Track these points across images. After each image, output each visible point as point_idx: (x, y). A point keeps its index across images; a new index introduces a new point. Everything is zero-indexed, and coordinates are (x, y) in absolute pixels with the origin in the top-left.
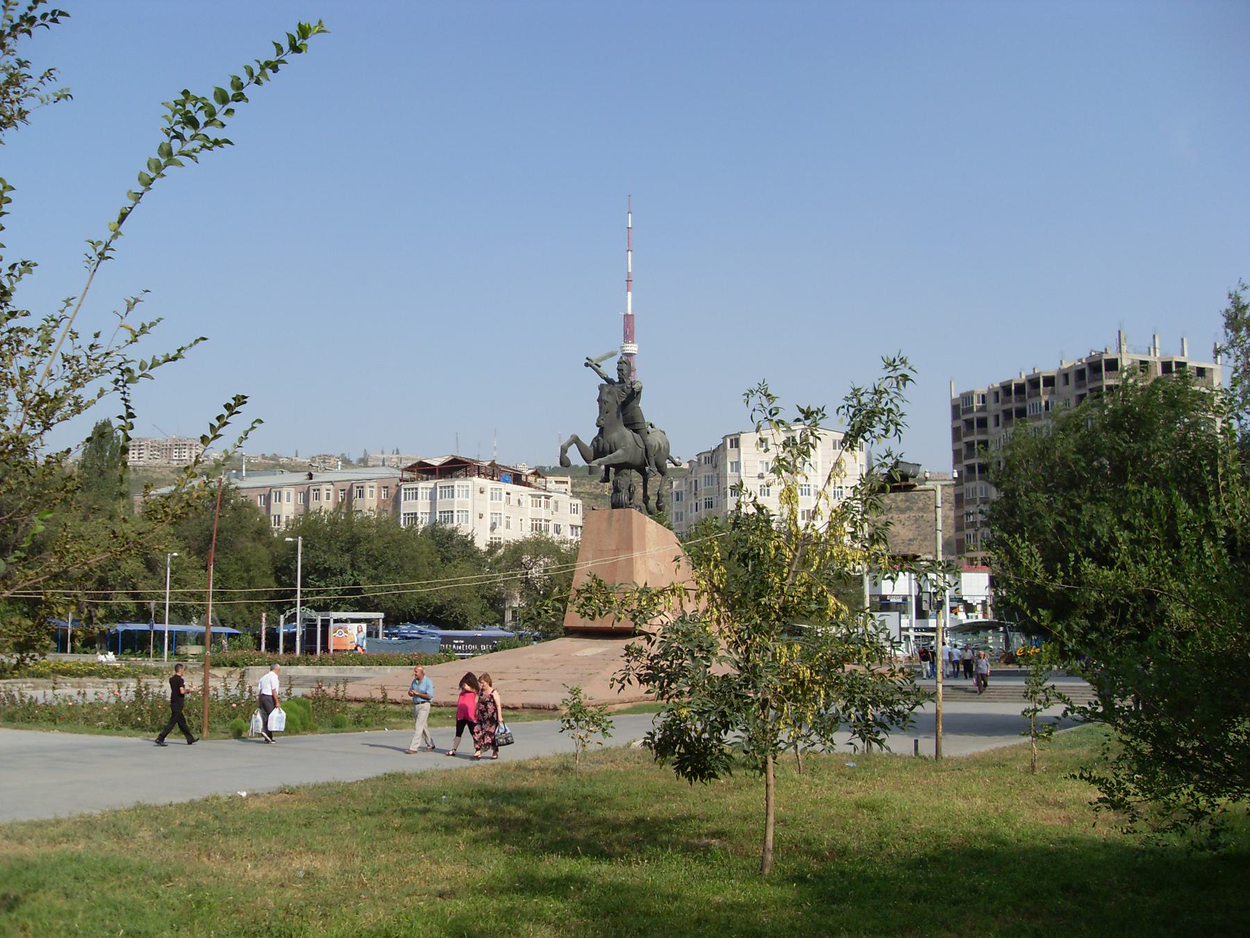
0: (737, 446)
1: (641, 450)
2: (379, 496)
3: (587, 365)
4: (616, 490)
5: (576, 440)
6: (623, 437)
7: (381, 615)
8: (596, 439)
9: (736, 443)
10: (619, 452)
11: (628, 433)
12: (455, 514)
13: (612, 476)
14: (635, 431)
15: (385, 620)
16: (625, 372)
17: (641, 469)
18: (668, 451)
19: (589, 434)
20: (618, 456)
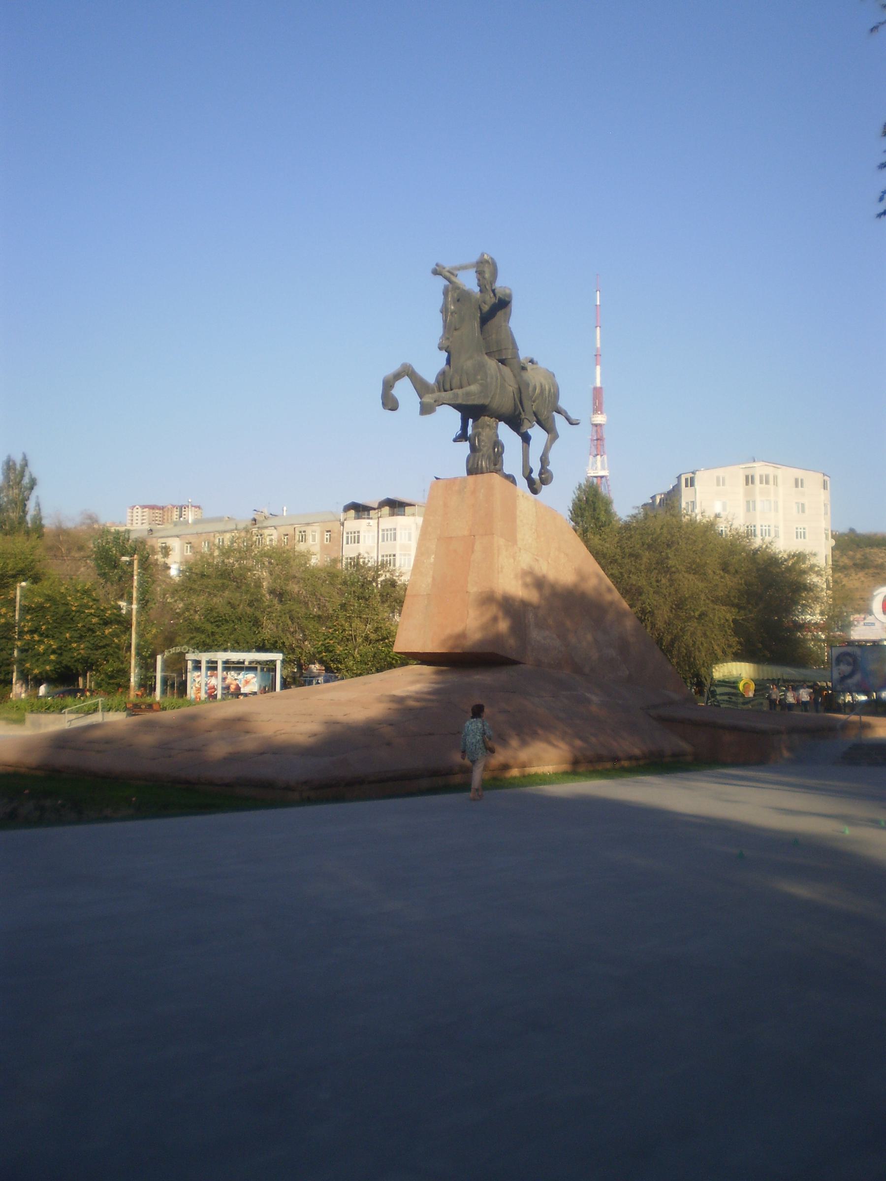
0: (692, 485)
1: (511, 387)
2: (322, 540)
3: (436, 272)
4: (473, 449)
5: (407, 372)
6: (481, 367)
7: (278, 657)
8: (443, 373)
9: (691, 483)
10: (474, 388)
11: (492, 364)
12: (398, 558)
13: (470, 431)
14: (503, 362)
15: (283, 662)
16: (487, 275)
17: (515, 423)
18: (556, 396)
19: (432, 365)
20: (473, 392)
